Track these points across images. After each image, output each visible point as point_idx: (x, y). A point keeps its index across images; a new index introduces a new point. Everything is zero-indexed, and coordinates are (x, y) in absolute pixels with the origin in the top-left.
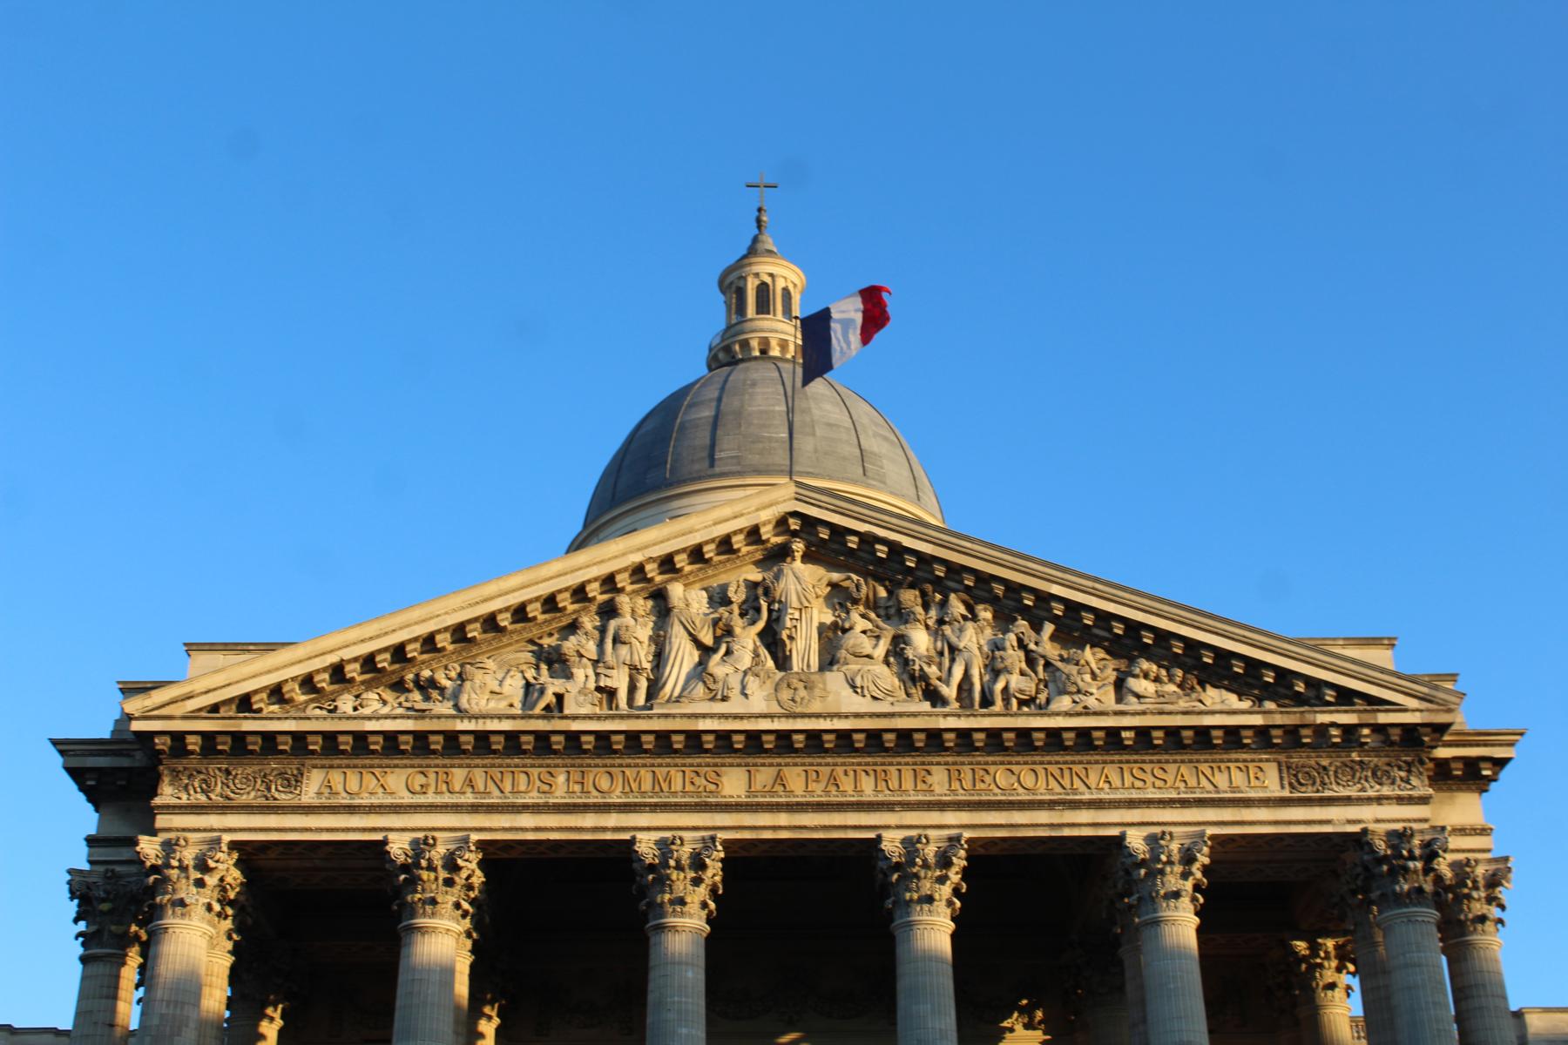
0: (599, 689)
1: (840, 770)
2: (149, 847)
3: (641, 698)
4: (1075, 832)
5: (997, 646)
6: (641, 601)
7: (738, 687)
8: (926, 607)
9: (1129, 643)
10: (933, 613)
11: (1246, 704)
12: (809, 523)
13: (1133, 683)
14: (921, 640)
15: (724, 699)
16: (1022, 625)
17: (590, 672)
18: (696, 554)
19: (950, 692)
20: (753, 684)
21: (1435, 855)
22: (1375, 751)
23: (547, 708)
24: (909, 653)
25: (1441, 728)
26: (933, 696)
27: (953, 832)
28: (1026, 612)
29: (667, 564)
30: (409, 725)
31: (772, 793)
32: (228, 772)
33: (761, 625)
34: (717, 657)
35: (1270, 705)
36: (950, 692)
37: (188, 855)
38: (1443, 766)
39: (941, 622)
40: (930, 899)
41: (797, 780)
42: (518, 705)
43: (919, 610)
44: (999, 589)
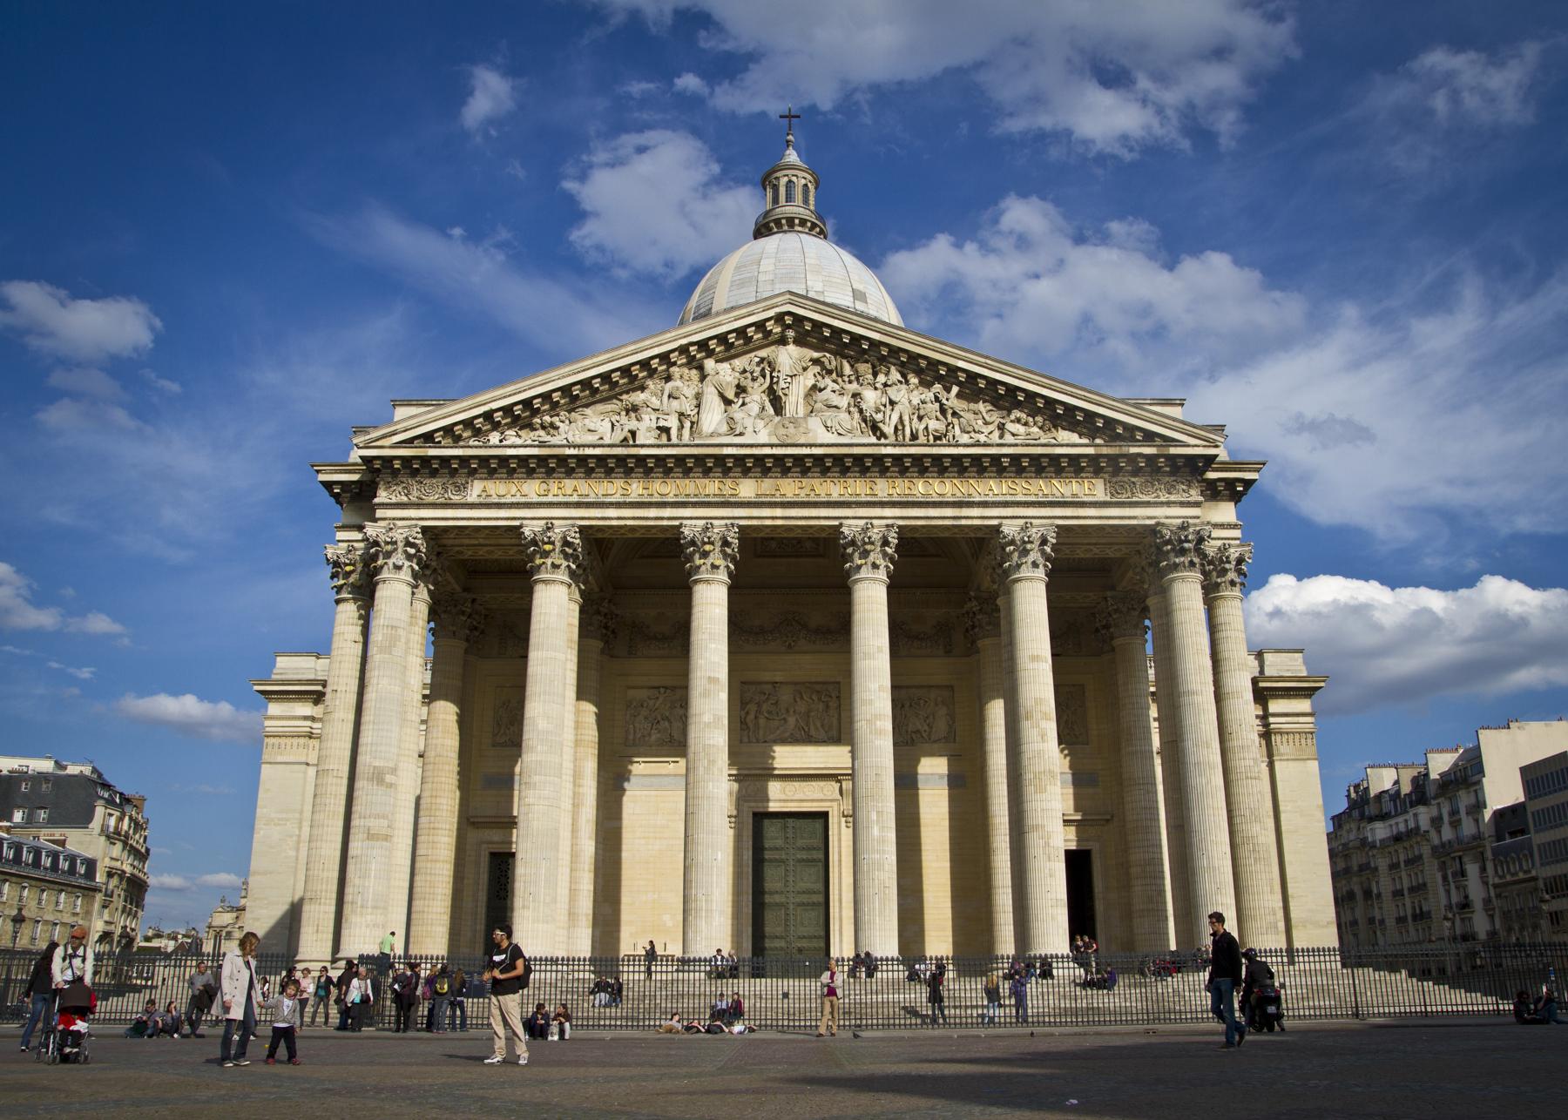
1: (816, 482)
3: (686, 432)
4: (969, 522)
6: (686, 370)
7: (750, 429)
8: (875, 375)
9: (1006, 399)
10: (881, 378)
11: (1085, 441)
12: (799, 320)
13: (1010, 427)
14: (871, 398)
15: (741, 434)
17: (654, 418)
19: (888, 430)
20: (760, 424)
21: (1201, 540)
22: (1172, 474)
23: (625, 439)
25: (1209, 460)
27: (890, 522)
28: (940, 379)
29: (703, 345)
34: (735, 407)
35: (1098, 441)
39: (885, 385)
41: (790, 488)
44: (923, 363)
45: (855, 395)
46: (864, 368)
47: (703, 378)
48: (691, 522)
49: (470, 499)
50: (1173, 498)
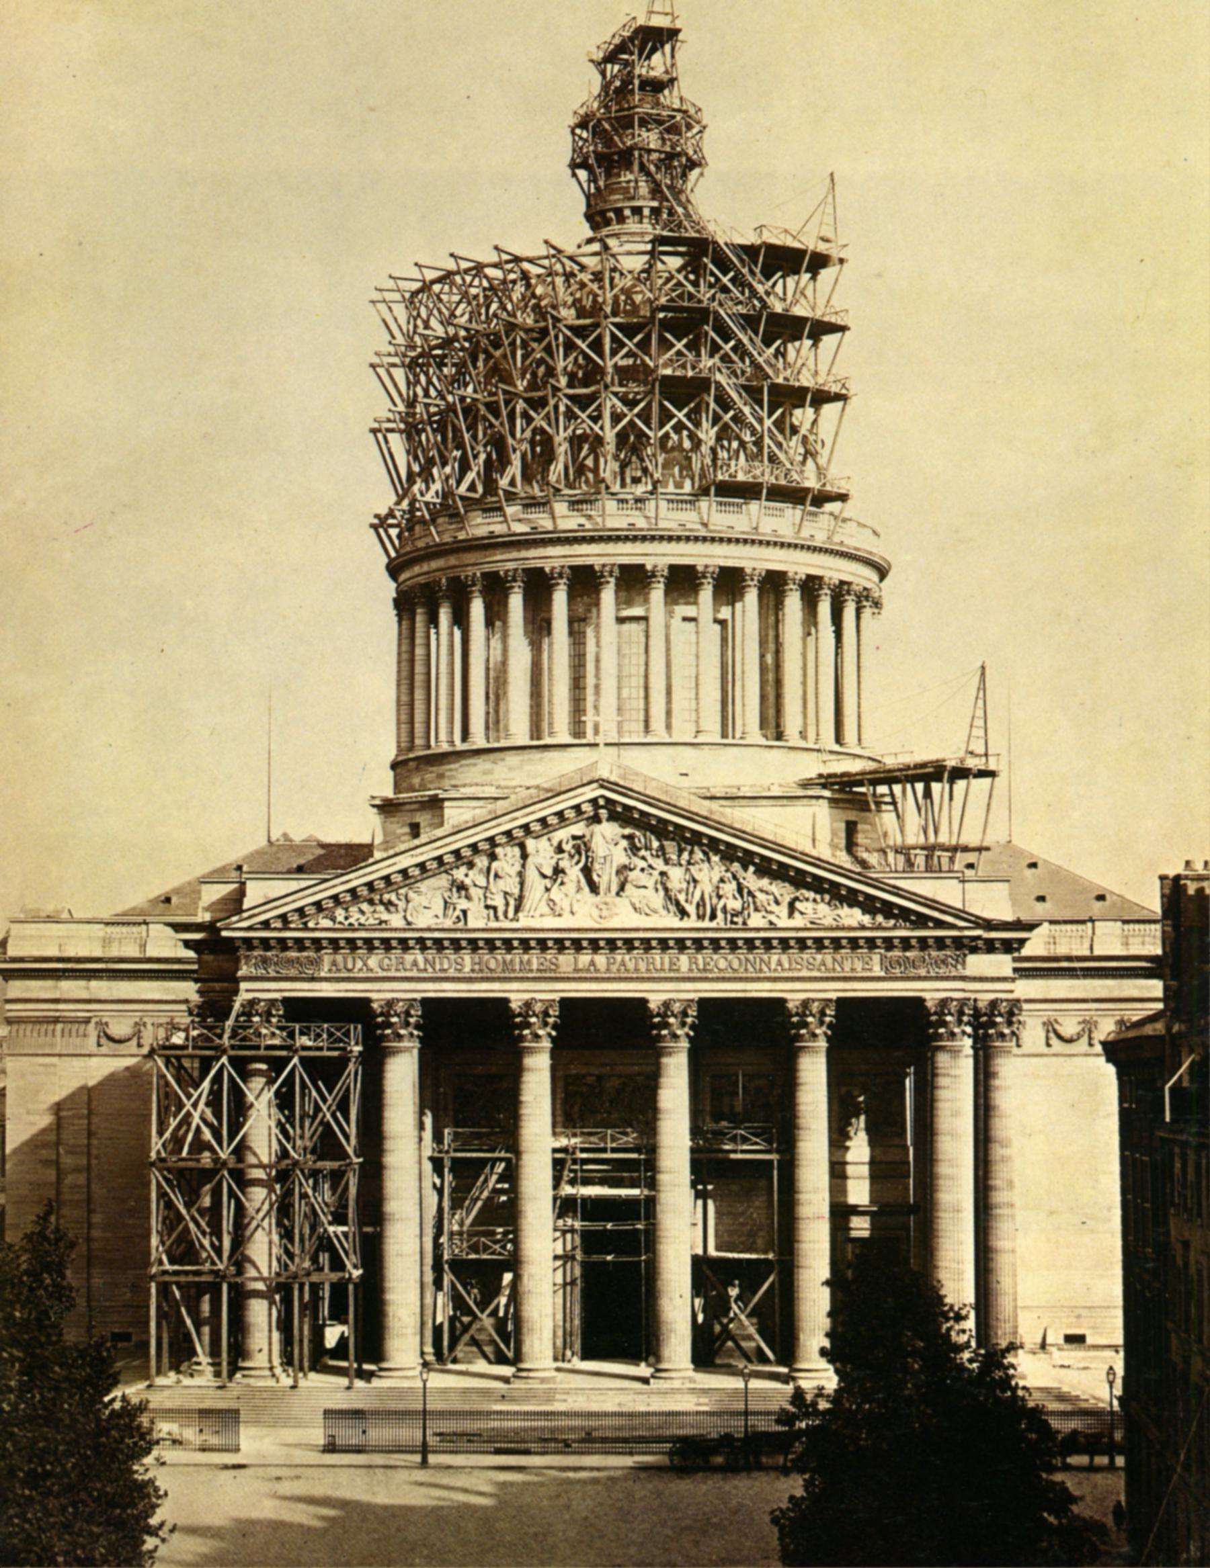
0: (487, 907)
5: (722, 880)
6: (508, 849)
7: (568, 909)
8: (681, 851)
10: (685, 855)
11: (866, 920)
13: (798, 905)
14: (677, 875)
15: (560, 915)
16: (736, 866)
19: (691, 909)
23: (458, 917)
24: (669, 885)
26: (683, 913)
28: (738, 860)
29: (526, 828)
31: (588, 970)
33: (581, 865)
39: (689, 863)
42: (441, 914)
43: (674, 857)
45: (663, 874)
47: (524, 856)
49: (323, 974)
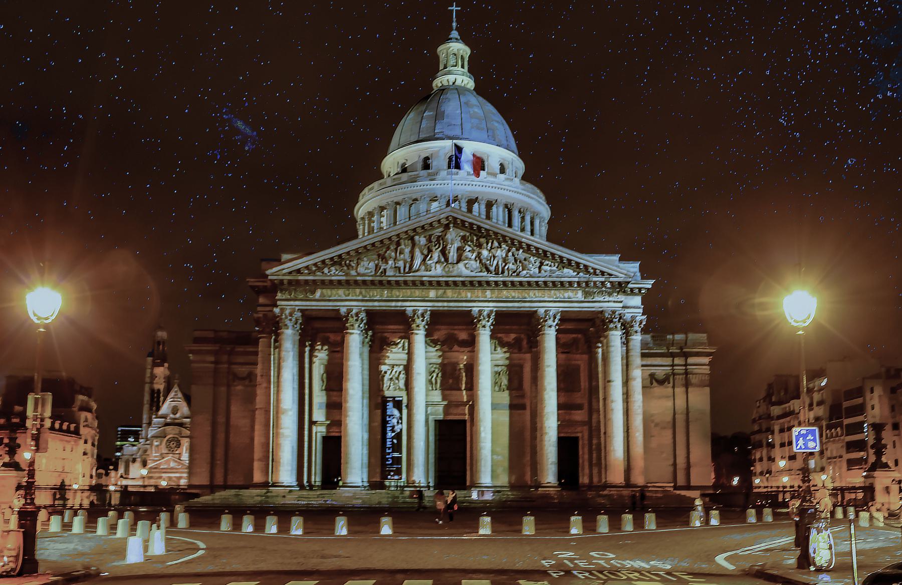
2: (277, 310)
3: (407, 270)
5: (507, 255)
12: (455, 219)
14: (485, 253)
18: (423, 227)
19: (492, 269)
30: (344, 278)
32: (295, 290)
35: (581, 274)
36: (492, 269)
37: (287, 312)
38: (632, 290)
39: (491, 248)
40: (484, 326)
41: (450, 293)
46: (482, 240)
47: (414, 245)
48: (409, 307)
50: (611, 299)
